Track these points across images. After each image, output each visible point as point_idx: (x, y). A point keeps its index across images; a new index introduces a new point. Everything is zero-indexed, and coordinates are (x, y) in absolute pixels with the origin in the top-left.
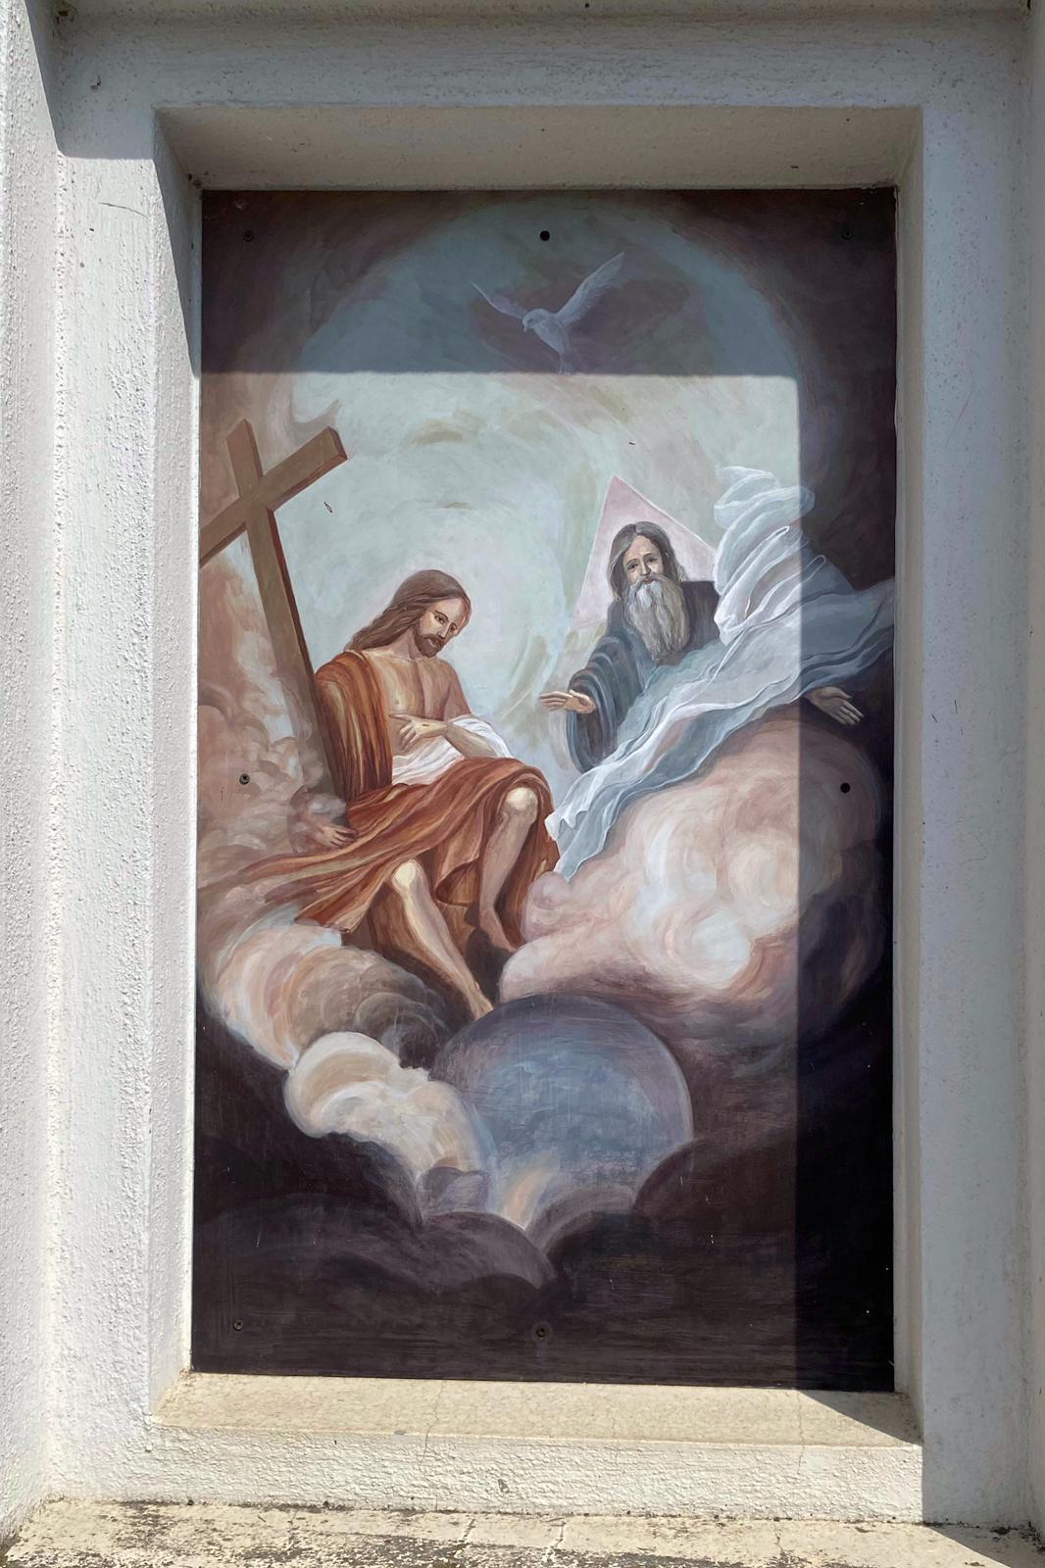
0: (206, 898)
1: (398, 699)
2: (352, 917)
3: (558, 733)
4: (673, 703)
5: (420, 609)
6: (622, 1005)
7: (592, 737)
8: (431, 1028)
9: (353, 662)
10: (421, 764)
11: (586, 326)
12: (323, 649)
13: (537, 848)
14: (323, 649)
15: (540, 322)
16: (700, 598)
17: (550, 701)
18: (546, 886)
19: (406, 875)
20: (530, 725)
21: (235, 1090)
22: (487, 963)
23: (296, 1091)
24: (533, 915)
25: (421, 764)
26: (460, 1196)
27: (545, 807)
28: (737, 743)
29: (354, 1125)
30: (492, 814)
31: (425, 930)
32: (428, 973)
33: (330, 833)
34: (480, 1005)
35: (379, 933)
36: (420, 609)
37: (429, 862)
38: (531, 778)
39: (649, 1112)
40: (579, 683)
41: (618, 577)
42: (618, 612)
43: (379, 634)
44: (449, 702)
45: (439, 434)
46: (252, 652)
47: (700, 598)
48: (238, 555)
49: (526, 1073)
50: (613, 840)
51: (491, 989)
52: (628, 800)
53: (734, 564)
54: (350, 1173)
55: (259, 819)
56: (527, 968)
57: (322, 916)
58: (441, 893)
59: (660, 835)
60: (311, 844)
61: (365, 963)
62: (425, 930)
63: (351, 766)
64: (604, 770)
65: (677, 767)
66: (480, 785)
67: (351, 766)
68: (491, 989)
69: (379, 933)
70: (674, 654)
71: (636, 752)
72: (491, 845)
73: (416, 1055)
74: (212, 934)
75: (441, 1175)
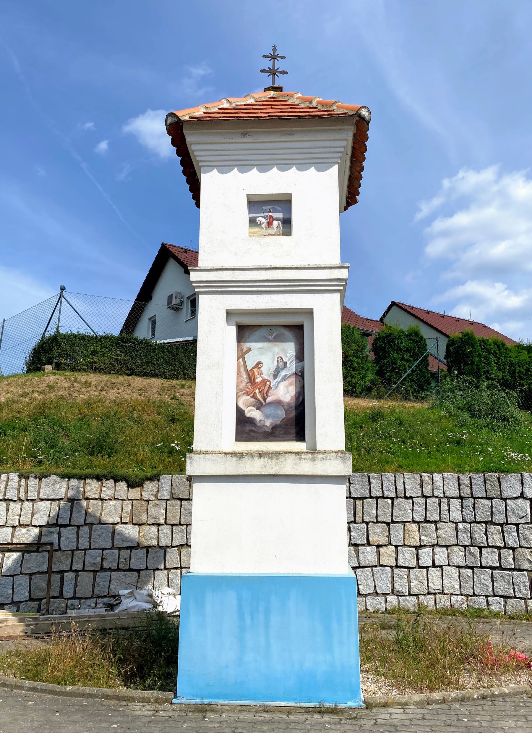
0: (237, 394)
1: (256, 373)
2: (251, 395)
3: (272, 376)
4: (283, 373)
5: (258, 365)
6: (278, 403)
7: (275, 377)
8: (259, 406)
9: (252, 370)
10: (258, 380)
11: (274, 338)
13: (270, 388)
15: (270, 337)
16: (285, 363)
17: (271, 373)
19: (257, 391)
20: (269, 376)
21: (240, 412)
22: (265, 399)
23: (246, 413)
24: (269, 394)
25: (258, 380)
26: (262, 423)
27: (270, 384)
28: (289, 377)
29: (252, 416)
30: (265, 384)
32: (259, 400)
33: (249, 387)
34: (264, 404)
35: (254, 397)
36: (258, 365)
37: (259, 389)
38: (269, 381)
39: (281, 414)
40: (274, 372)
41: (278, 361)
43: (254, 367)
44: (261, 373)
45: (260, 348)
46: (242, 369)
47: (285, 363)
48: (241, 360)
49: (269, 410)
50: (277, 387)
51: (265, 402)
52: (279, 383)
53: (289, 360)
54: (251, 421)
55: (242, 386)
56: (269, 400)
57: (249, 395)
58: (260, 392)
59: (282, 386)
60: (248, 388)
61: (253, 400)
63: (252, 380)
64: (276, 380)
65: (284, 379)
66: (264, 382)
67: (252, 380)
68: (265, 402)
69: (254, 397)
70: (283, 369)
71: (279, 379)
72: (265, 388)
73: (258, 409)
74: (238, 397)
75: (260, 421)
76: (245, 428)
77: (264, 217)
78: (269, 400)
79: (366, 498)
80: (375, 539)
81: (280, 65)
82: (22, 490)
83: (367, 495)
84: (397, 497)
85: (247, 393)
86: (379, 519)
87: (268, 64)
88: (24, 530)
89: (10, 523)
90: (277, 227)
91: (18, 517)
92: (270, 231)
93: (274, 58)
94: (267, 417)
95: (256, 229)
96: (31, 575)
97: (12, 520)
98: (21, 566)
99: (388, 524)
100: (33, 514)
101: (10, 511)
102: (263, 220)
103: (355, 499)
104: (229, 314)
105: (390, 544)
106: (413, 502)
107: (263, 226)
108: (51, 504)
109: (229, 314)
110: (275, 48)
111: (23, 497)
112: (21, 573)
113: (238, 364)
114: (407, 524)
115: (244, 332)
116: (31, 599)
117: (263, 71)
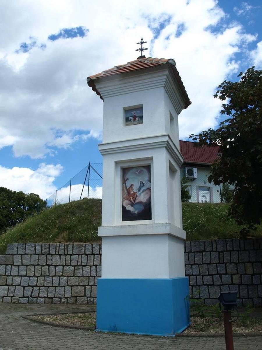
0: (123, 200)
2: (129, 200)
3: (138, 190)
4: (143, 189)
5: (132, 186)
6: (141, 203)
7: (139, 191)
8: (132, 205)
9: (129, 188)
10: (132, 193)
11: (139, 173)
12: (128, 188)
13: (137, 196)
14: (128, 188)
15: (137, 172)
16: (144, 184)
17: (137, 189)
18: (137, 198)
19: (131, 198)
20: (137, 190)
21: (124, 208)
22: (135, 201)
23: (126, 208)
24: (137, 199)
25: (132, 193)
26: (134, 212)
27: (137, 194)
28: (145, 190)
29: (129, 209)
30: (135, 194)
31: (132, 200)
32: (132, 202)
33: (128, 196)
34: (134, 203)
36: (132, 186)
37: (132, 197)
38: (136, 193)
39: (142, 208)
40: (139, 188)
41: (140, 184)
42: (140, 185)
43: (130, 187)
44: (133, 190)
45: (133, 178)
46: (125, 189)
47: (144, 184)
48: (124, 184)
49: (136, 206)
50: (140, 195)
51: (135, 202)
52: (141, 193)
53: (145, 182)
54: (129, 211)
55: (125, 196)
56: (136, 202)
57: (128, 200)
58: (133, 198)
59: (142, 195)
60: (127, 197)
61: (129, 202)
62: (132, 200)
63: (129, 193)
64: (140, 192)
65: (143, 192)
66: (134, 193)
67: (129, 193)
68: (135, 202)
69: (130, 201)
70: (143, 186)
71: (141, 191)
73: (131, 206)
74: (123, 201)
75: (133, 211)
76: (127, 216)
77: (132, 117)
78: (136, 202)
79: (225, 251)
80: (229, 271)
81: (145, 46)
82: (66, 250)
83: (225, 250)
84: (241, 250)
85: (127, 199)
86: (232, 261)
87: (139, 46)
88: (68, 267)
89: (61, 264)
90: (138, 121)
91: (65, 262)
92: (135, 123)
93: (142, 43)
94: (136, 209)
95: (129, 123)
96: (72, 286)
97: (63, 263)
98: (67, 282)
99: (236, 264)
100: (71, 261)
101: (61, 259)
102: (131, 118)
103: (219, 252)
104: (117, 163)
105: (238, 274)
106: (249, 252)
107: (132, 120)
108: (78, 256)
109: (117, 163)
110: (142, 39)
111: (66, 253)
112: (68, 285)
113: (123, 186)
114: (246, 263)
115: (125, 171)
116: (72, 297)
117: (137, 50)
